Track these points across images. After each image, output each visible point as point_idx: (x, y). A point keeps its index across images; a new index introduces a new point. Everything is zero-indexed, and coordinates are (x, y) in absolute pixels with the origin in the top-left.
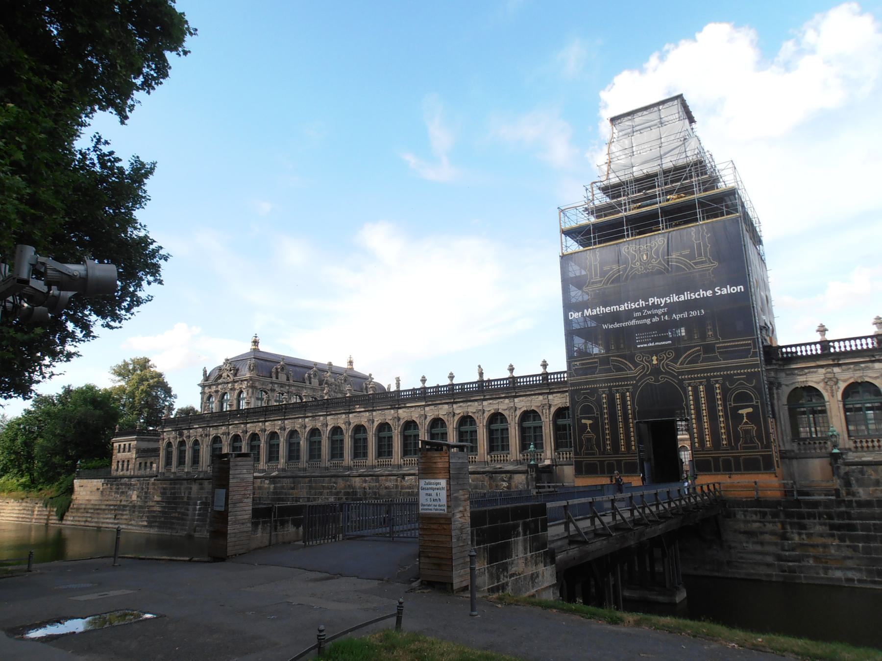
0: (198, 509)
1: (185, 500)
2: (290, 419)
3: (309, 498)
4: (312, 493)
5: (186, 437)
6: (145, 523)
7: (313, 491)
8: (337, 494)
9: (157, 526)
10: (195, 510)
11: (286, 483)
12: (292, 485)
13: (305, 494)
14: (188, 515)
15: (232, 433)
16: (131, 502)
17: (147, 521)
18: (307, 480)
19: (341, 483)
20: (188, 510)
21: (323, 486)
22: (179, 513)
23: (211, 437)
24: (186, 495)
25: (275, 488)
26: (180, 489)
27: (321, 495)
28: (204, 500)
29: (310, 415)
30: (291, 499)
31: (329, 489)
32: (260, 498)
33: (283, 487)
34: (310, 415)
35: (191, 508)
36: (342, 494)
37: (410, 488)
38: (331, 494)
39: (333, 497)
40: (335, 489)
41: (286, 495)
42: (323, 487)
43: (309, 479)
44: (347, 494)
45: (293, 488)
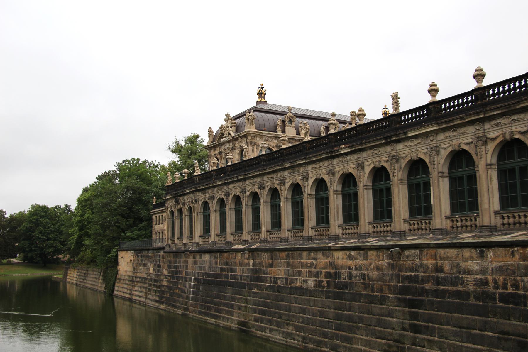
2: (268, 173)
3: (286, 279)
4: (290, 272)
5: (182, 204)
7: (291, 270)
8: (317, 275)
11: (265, 258)
12: (270, 261)
13: (283, 273)
15: (217, 197)
18: (284, 254)
19: (322, 260)
21: (302, 263)
23: (200, 203)
25: (254, 264)
27: (300, 276)
28: (197, 277)
29: (288, 165)
30: (269, 279)
31: (307, 267)
33: (261, 264)
34: (288, 165)
36: (323, 275)
37: (412, 270)
38: (310, 274)
39: (312, 279)
40: (315, 268)
41: (264, 274)
42: (302, 265)
43: (286, 252)
44: (328, 275)
45: (271, 265)
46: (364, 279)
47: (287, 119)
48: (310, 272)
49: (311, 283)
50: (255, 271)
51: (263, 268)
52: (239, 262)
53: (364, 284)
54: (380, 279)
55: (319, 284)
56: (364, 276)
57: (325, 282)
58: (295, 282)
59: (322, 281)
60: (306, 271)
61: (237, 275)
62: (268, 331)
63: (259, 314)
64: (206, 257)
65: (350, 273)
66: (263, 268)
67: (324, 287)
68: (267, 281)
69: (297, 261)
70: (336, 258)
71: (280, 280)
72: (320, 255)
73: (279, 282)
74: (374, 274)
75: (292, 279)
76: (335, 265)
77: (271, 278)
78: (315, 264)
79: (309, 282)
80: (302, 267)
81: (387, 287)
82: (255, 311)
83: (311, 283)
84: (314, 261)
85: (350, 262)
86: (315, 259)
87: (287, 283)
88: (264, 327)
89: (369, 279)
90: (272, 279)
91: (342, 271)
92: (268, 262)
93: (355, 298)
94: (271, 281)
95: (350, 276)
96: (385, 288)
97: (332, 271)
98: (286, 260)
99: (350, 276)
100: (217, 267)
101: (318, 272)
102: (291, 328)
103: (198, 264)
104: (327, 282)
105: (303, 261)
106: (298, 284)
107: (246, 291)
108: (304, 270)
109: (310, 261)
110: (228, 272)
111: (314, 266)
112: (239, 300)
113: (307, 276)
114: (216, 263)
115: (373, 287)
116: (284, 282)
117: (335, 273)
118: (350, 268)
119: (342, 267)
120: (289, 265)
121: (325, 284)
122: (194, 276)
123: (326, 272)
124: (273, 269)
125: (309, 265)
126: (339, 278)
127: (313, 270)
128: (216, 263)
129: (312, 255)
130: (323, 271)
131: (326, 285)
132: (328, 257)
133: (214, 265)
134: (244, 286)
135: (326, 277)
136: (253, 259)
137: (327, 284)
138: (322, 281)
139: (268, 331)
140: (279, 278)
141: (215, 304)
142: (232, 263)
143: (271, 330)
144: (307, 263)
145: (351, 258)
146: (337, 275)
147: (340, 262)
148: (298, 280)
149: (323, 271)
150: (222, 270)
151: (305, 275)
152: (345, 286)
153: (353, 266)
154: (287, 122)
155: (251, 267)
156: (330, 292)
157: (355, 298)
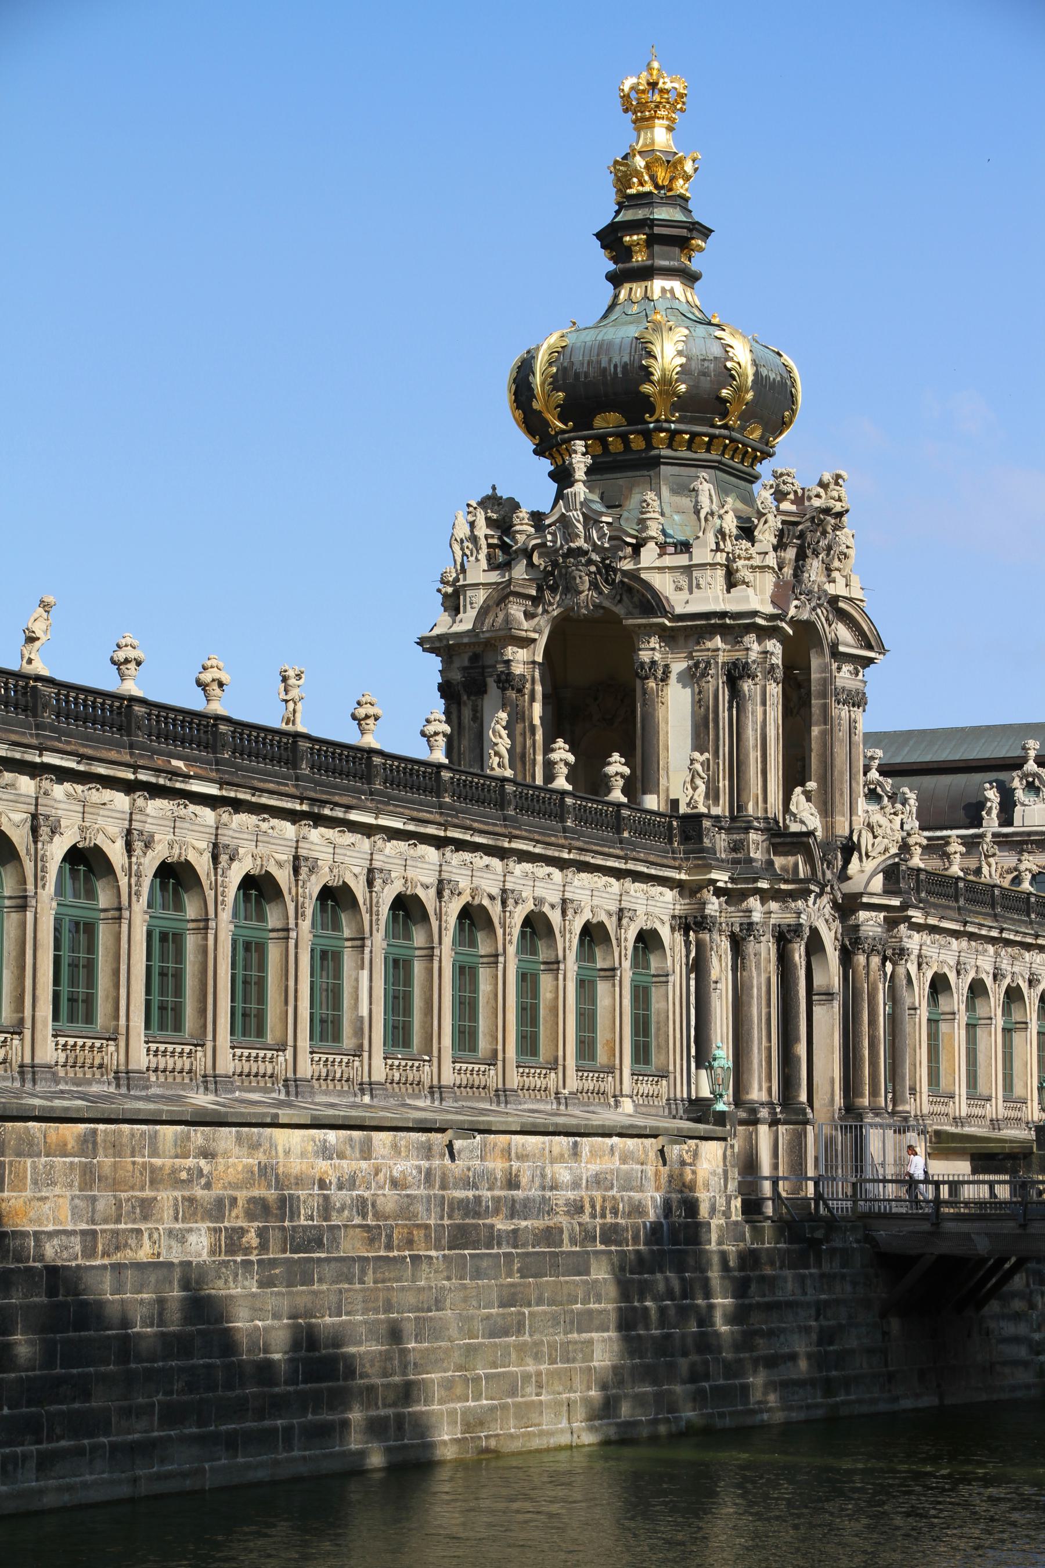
8: (218, 1209)
13: (66, 1213)
21: (154, 1169)
27: (145, 1218)
31: (178, 1183)
36: (238, 1211)
38: (191, 1208)
39: (204, 1226)
40: (208, 1186)
42: (155, 1178)
44: (259, 1209)
46: (364, 1216)
48: (191, 1200)
53: (367, 1228)
54: (405, 1210)
55: (233, 1241)
56: (361, 1206)
57: (252, 1234)
58: (132, 1242)
59: (242, 1231)
60: (176, 1199)
65: (326, 1198)
67: (247, 1251)
69: (134, 1163)
70: (280, 1149)
71: (56, 1242)
74: (388, 1199)
75: (116, 1233)
76: (277, 1175)
78: (205, 1172)
79: (192, 1238)
80: (154, 1183)
81: (422, 1232)
84: (202, 1162)
85: (323, 1166)
86: (207, 1154)
87: (90, 1252)
89: (377, 1215)
91: (302, 1193)
95: (326, 1208)
96: (418, 1235)
97: (271, 1194)
98: (76, 1160)
99: (326, 1208)
101: (219, 1202)
104: (262, 1233)
105: (157, 1161)
106: (144, 1253)
108: (166, 1197)
109: (190, 1162)
111: (203, 1181)
113: (176, 1219)
115: (390, 1237)
116: (78, 1248)
117: (282, 1200)
118: (322, 1184)
119: (299, 1181)
120: (89, 1177)
121: (252, 1238)
123: (252, 1200)
125: (184, 1175)
126: (294, 1215)
127: (199, 1192)
130: (242, 1195)
131: (255, 1242)
135: (250, 1216)
137: (258, 1240)
138: (242, 1231)
143: (45, 1463)
144: (174, 1171)
145: (325, 1152)
146: (287, 1206)
147: (296, 1166)
148: (146, 1235)
151: (168, 1214)
152: (313, 1240)
153: (332, 1178)
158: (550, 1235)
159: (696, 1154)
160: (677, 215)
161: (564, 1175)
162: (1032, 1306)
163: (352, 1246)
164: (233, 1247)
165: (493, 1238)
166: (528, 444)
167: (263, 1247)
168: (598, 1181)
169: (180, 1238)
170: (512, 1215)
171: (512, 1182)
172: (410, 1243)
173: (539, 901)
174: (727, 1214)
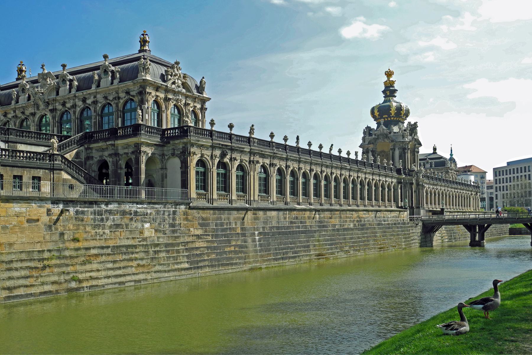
0: (257, 240)
1: (239, 231)
3: (341, 225)
6: (186, 266)
8: (354, 221)
9: (208, 266)
10: (254, 241)
13: (338, 222)
14: (247, 247)
16: (145, 239)
17: (188, 262)
19: (355, 215)
20: (245, 242)
22: (235, 246)
24: (239, 225)
26: (229, 219)
30: (331, 226)
32: (311, 226)
35: (249, 240)
39: (352, 223)
41: (327, 223)
44: (358, 221)
45: (331, 218)
47: (426, 162)
48: (351, 220)
49: (352, 226)
50: (320, 222)
51: (326, 220)
52: (308, 217)
53: (369, 223)
55: (355, 225)
61: (308, 225)
62: (336, 253)
63: (329, 246)
64: (274, 213)
66: (326, 220)
68: (330, 227)
72: (354, 213)
73: (337, 227)
77: (332, 225)
80: (347, 218)
82: (326, 245)
83: (352, 226)
85: (364, 216)
86: (352, 214)
88: (334, 252)
90: (333, 226)
91: (362, 219)
92: (329, 216)
93: (367, 229)
94: (332, 227)
95: (365, 221)
97: (359, 219)
99: (365, 221)
100: (286, 221)
102: (347, 248)
103: (261, 219)
104: (358, 224)
106: (346, 227)
107: (316, 235)
108: (348, 220)
109: (350, 215)
110: (298, 224)
112: (313, 241)
114: (285, 218)
117: (360, 220)
119: (362, 218)
121: (357, 225)
122: (257, 231)
124: (333, 220)
127: (351, 219)
128: (285, 218)
129: (351, 212)
132: (357, 213)
133: (282, 220)
134: (315, 232)
135: (357, 222)
136: (319, 215)
139: (336, 253)
140: (337, 225)
141: (292, 248)
142: (301, 218)
146: (361, 221)
147: (361, 216)
149: (356, 219)
150: (291, 223)
152: (364, 225)
154: (426, 163)
155: (317, 220)
156: (359, 228)
157: (367, 229)
158: (388, 224)
159: (404, 213)
160: (393, 89)
161: (390, 216)
162: (441, 232)
163: (368, 226)
164: (355, 226)
165: (382, 225)
166: (373, 119)
167: (358, 226)
168: (393, 217)
169: (350, 225)
170: (384, 221)
171: (384, 217)
172: (373, 225)
173: (383, 181)
174: (407, 221)
